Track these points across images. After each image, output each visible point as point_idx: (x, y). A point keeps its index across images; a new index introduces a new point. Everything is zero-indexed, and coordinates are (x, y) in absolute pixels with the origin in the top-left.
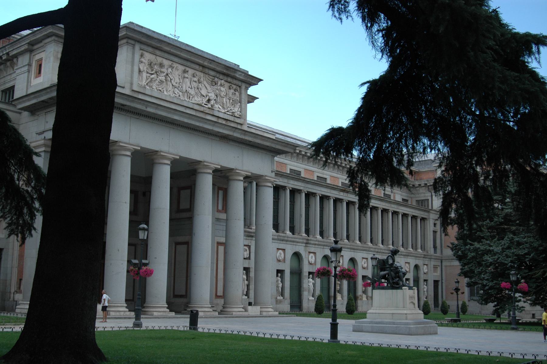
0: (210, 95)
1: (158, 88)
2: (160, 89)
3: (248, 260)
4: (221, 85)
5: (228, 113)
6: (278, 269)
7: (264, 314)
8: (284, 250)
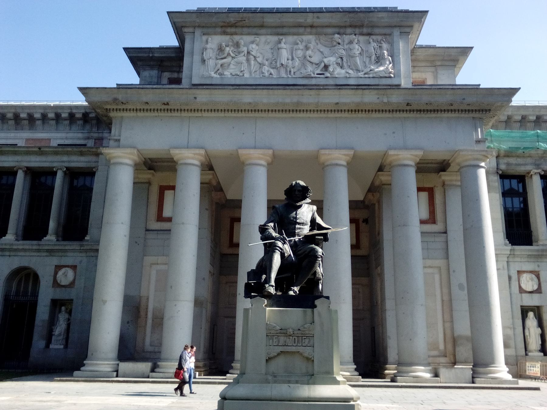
0: (326, 60)
1: (234, 74)
5: (366, 76)
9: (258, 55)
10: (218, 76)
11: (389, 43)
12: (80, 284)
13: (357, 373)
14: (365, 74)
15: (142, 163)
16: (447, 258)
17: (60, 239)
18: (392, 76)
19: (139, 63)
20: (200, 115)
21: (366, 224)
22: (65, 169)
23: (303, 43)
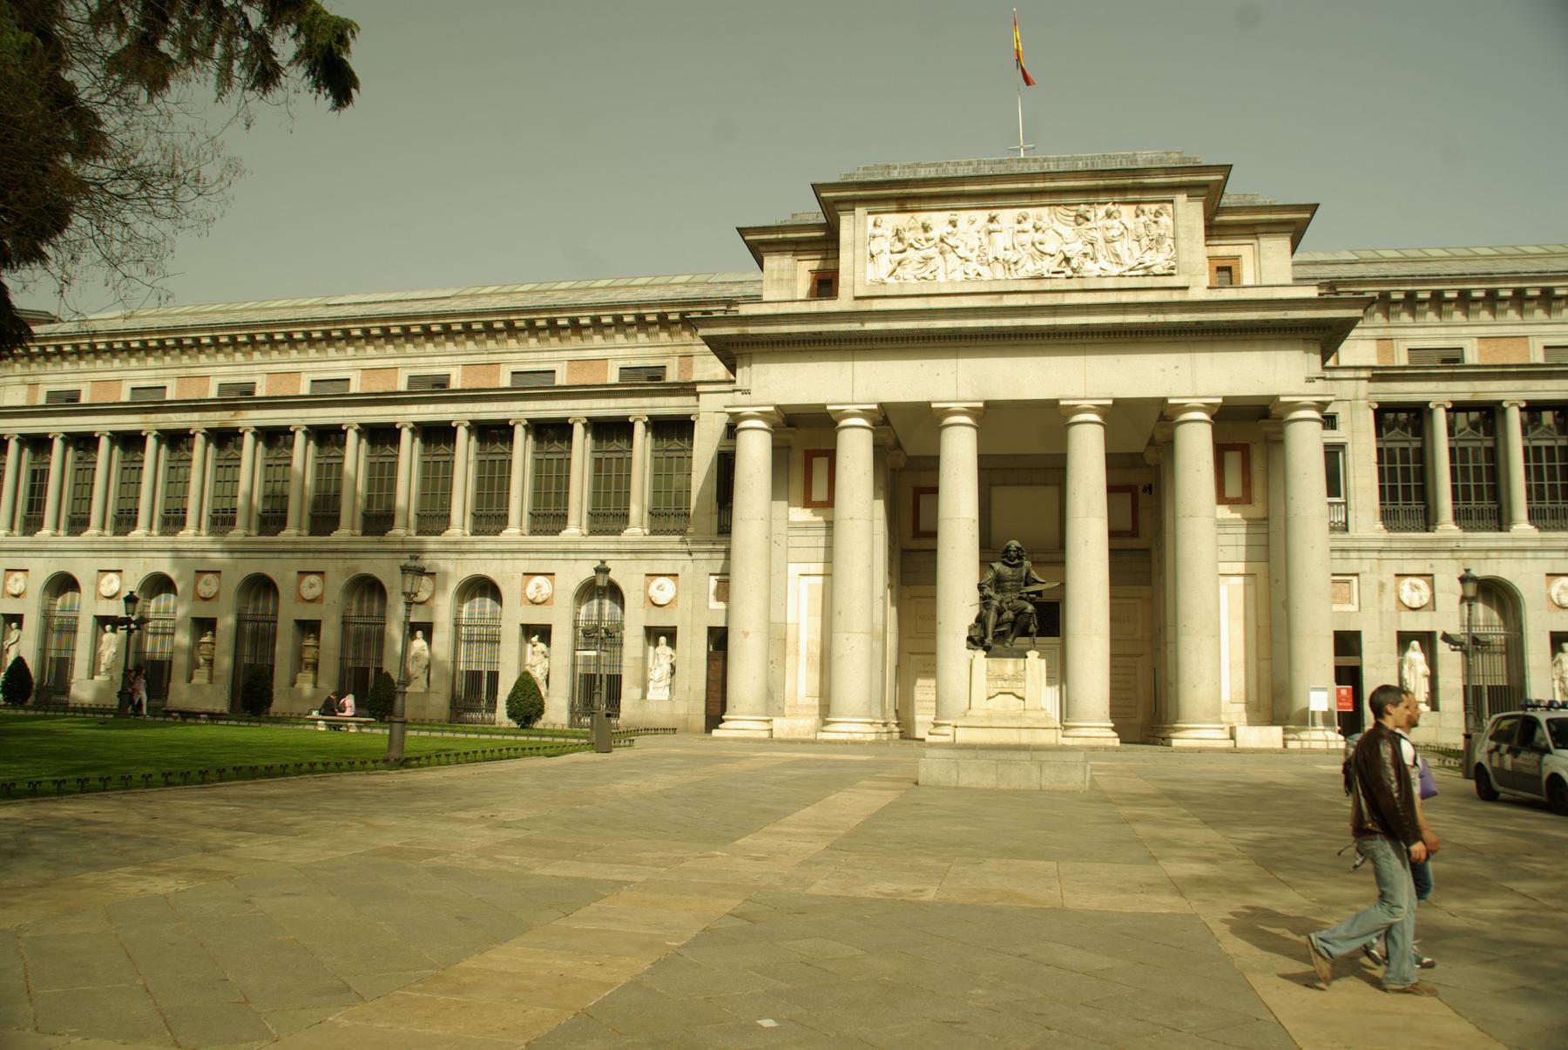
0: (1065, 248)
1: (919, 276)
2: (925, 275)
4: (1109, 215)
6: (1555, 629)
7: (1291, 745)
9: (958, 243)
10: (896, 282)
11: (1168, 215)
12: (685, 602)
13: (1115, 734)
14: (1130, 270)
15: (781, 421)
16: (1268, 560)
17: (647, 531)
18: (1175, 272)
19: (762, 248)
20: (870, 347)
21: (1150, 493)
22: (646, 419)
23: (1028, 220)
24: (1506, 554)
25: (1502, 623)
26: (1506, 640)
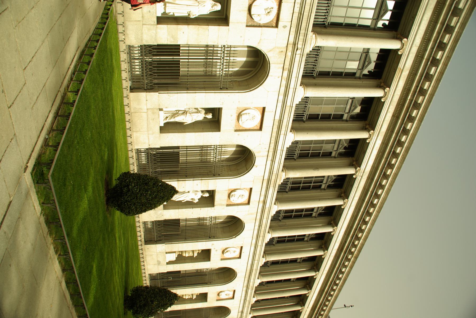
3: (245, 21)
8: (261, 129)
24: (284, 83)
25: (230, 73)
26: (215, 76)
